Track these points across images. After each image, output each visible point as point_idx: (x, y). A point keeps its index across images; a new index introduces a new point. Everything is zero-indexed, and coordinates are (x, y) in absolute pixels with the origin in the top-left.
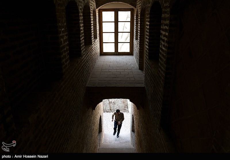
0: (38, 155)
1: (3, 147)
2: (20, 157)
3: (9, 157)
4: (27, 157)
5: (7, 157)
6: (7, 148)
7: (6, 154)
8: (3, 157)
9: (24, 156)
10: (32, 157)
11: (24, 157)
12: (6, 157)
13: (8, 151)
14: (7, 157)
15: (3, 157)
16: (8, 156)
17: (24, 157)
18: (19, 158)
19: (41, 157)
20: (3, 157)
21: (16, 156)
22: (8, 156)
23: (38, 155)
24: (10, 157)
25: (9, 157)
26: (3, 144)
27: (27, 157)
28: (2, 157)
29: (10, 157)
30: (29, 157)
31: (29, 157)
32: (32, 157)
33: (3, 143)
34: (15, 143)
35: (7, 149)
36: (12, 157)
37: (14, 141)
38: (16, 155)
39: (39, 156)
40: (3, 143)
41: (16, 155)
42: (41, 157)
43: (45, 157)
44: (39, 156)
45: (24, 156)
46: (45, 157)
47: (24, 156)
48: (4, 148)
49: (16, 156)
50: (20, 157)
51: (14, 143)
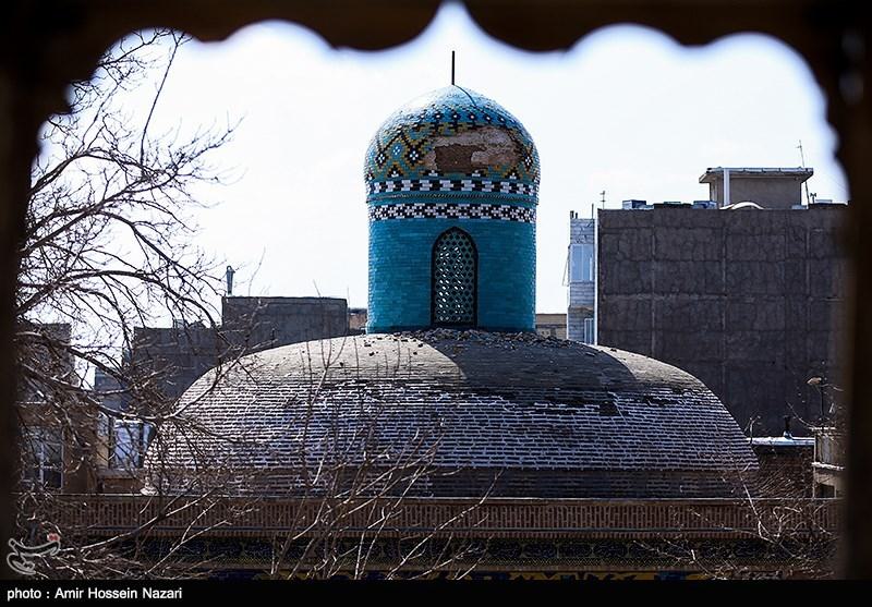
0: (145, 590)
1: (12, 558)
2: (77, 594)
3: (33, 594)
4: (102, 594)
5: (26, 594)
6: (28, 563)
7: (25, 583)
8: (12, 594)
9: (93, 590)
10: (123, 594)
11: (93, 596)
12: (22, 595)
13: (29, 571)
14: (26, 594)
15: (12, 594)
16: (32, 591)
17: (93, 596)
18: (70, 601)
19: (156, 595)
20: (11, 594)
21: (59, 592)
22: (32, 591)
23: (145, 590)
24: (38, 594)
25: (33, 594)
26: (13, 547)
27: (102, 594)
28: (9, 597)
29: (38, 594)
30: (108, 594)
31: (108, 594)
32: (123, 594)
33: (12, 543)
34: (55, 545)
35: (26, 566)
36: (44, 595)
37: (53, 535)
38: (60, 589)
39: (148, 593)
40: (12, 543)
41: (60, 589)
42: (156, 595)
43: (172, 594)
44: (148, 593)
45: (93, 590)
46: (172, 594)
47: (90, 593)
48: (14, 562)
49: (59, 592)
50: (77, 594)
51: (54, 541)
